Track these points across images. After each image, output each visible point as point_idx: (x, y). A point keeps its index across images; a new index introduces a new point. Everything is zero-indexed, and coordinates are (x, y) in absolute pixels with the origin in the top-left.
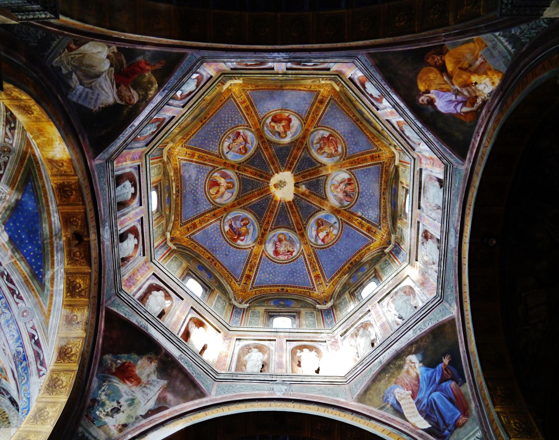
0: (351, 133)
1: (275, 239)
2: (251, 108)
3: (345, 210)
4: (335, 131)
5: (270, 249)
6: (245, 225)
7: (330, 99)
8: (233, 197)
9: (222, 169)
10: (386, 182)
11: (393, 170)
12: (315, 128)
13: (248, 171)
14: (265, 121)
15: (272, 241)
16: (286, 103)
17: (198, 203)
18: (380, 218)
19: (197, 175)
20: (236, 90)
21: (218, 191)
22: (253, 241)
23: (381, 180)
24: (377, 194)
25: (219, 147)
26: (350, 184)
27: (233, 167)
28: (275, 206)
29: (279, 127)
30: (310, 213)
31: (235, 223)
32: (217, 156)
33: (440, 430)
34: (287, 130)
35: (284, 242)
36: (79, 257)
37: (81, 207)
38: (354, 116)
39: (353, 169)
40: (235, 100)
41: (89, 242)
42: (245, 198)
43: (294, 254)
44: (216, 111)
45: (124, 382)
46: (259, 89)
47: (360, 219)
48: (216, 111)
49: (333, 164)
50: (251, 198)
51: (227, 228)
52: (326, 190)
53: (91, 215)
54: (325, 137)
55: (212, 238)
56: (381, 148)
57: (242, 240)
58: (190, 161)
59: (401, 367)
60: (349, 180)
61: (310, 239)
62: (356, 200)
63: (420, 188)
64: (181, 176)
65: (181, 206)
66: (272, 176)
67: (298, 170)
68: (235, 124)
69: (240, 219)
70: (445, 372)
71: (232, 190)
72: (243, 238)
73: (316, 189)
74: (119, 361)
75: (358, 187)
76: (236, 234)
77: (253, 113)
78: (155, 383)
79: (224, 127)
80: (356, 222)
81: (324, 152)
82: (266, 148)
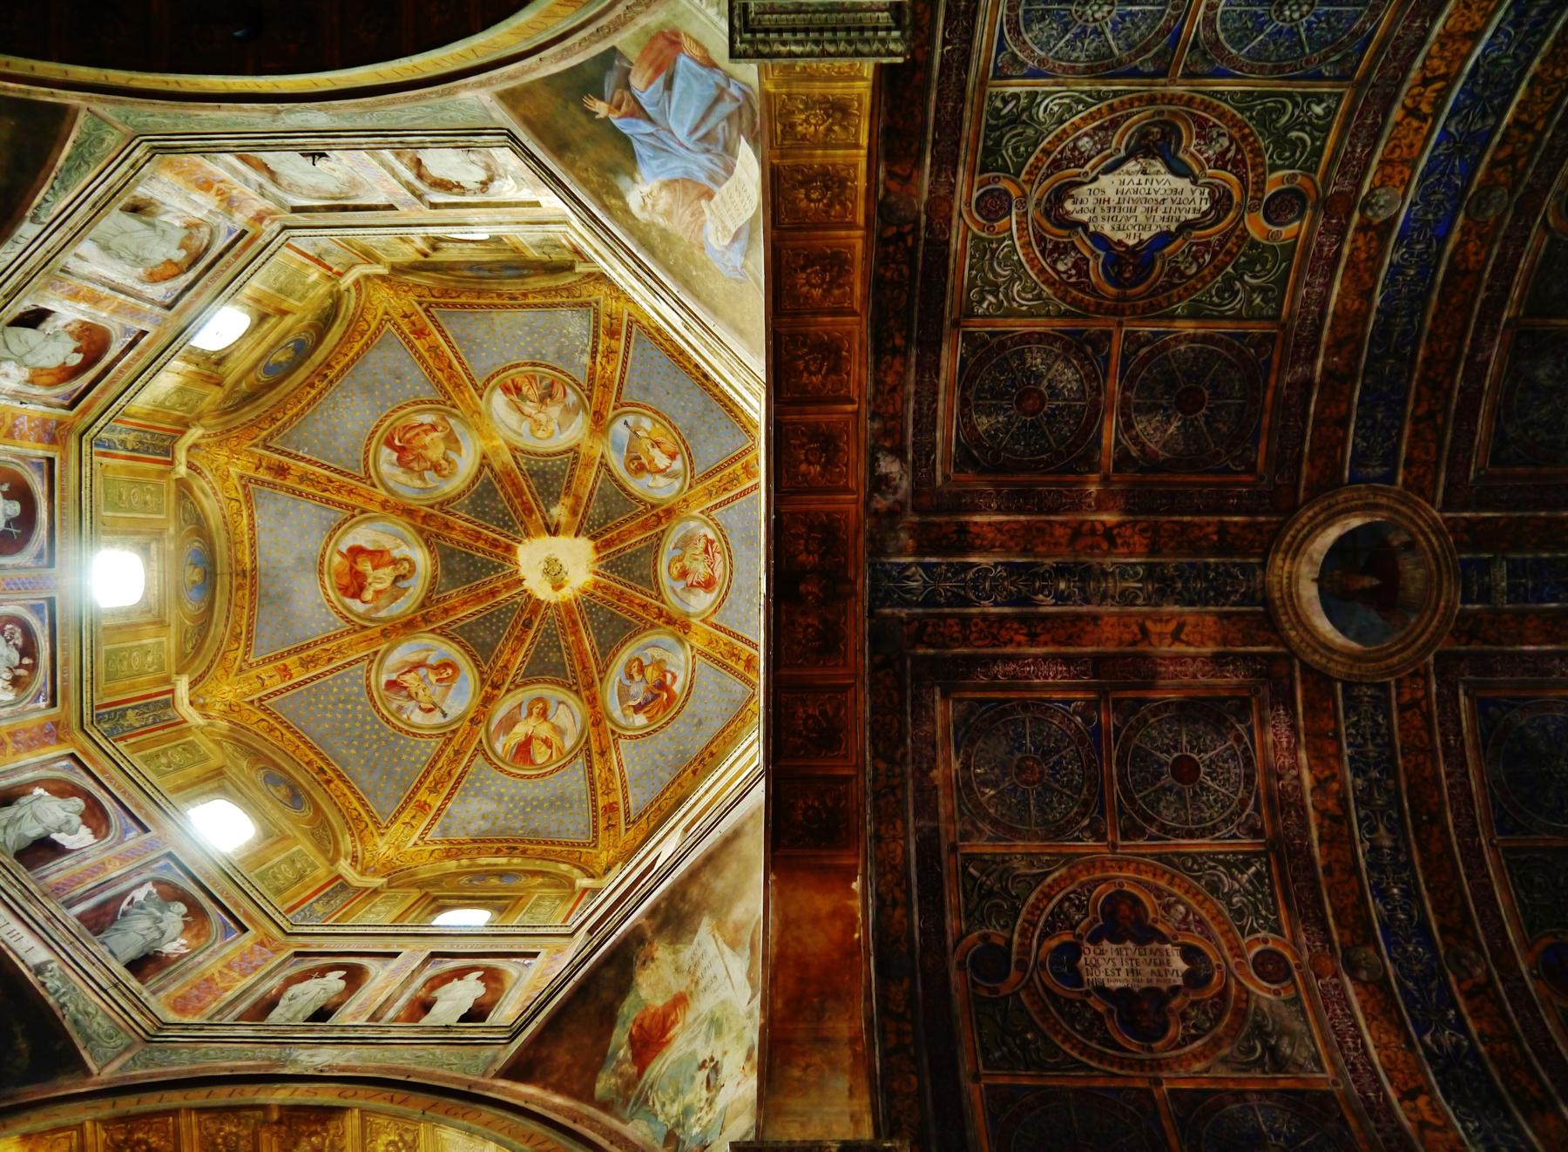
0: (368, 390)
1: (679, 586)
2: (311, 652)
3: (589, 398)
4: (373, 433)
5: (701, 602)
6: (641, 670)
7: (267, 448)
8: (570, 702)
9: (487, 730)
10: (480, 294)
11: (428, 278)
12: (374, 486)
13: (509, 661)
14: (358, 616)
15: (684, 595)
16: (300, 560)
17: (562, 798)
18: (576, 305)
19: (486, 796)
20: (226, 690)
21: (546, 742)
22: (678, 646)
23: (479, 306)
24: (521, 316)
25: (421, 736)
26: (518, 390)
27: (488, 700)
28: (606, 588)
29: (379, 580)
30: (618, 493)
31: (634, 698)
32: (446, 744)
33: (740, 108)
34: (386, 558)
35: (687, 563)
36: (324, 1139)
37: (182, 1121)
38: (312, 386)
39: (472, 380)
40: (275, 694)
41: (281, 1107)
42: (578, 668)
43: (711, 536)
44: (305, 742)
45: (668, 1042)
46: (249, 632)
47: (599, 358)
48: (305, 742)
49: (475, 434)
50: (581, 652)
51: (640, 720)
52: (550, 450)
53: (222, 1096)
54: (399, 459)
55: (654, 762)
56: (380, 312)
57: (674, 678)
58: (438, 814)
59: (665, 234)
60: (506, 390)
61: (674, 492)
62: (554, 369)
63: (345, 208)
64: (475, 841)
65: (553, 843)
66: (530, 596)
67: (510, 528)
68: (359, 695)
69: (627, 682)
70: (624, 108)
71: (552, 705)
72: (669, 676)
73: (557, 477)
74: (622, 1053)
75: (517, 366)
76: (658, 696)
77: (327, 646)
78: (699, 953)
79: (364, 723)
80: (609, 368)
81: (447, 460)
82: (446, 611)
